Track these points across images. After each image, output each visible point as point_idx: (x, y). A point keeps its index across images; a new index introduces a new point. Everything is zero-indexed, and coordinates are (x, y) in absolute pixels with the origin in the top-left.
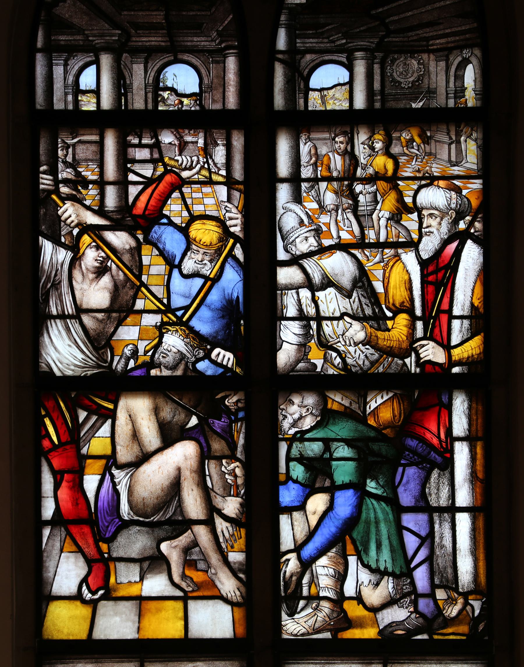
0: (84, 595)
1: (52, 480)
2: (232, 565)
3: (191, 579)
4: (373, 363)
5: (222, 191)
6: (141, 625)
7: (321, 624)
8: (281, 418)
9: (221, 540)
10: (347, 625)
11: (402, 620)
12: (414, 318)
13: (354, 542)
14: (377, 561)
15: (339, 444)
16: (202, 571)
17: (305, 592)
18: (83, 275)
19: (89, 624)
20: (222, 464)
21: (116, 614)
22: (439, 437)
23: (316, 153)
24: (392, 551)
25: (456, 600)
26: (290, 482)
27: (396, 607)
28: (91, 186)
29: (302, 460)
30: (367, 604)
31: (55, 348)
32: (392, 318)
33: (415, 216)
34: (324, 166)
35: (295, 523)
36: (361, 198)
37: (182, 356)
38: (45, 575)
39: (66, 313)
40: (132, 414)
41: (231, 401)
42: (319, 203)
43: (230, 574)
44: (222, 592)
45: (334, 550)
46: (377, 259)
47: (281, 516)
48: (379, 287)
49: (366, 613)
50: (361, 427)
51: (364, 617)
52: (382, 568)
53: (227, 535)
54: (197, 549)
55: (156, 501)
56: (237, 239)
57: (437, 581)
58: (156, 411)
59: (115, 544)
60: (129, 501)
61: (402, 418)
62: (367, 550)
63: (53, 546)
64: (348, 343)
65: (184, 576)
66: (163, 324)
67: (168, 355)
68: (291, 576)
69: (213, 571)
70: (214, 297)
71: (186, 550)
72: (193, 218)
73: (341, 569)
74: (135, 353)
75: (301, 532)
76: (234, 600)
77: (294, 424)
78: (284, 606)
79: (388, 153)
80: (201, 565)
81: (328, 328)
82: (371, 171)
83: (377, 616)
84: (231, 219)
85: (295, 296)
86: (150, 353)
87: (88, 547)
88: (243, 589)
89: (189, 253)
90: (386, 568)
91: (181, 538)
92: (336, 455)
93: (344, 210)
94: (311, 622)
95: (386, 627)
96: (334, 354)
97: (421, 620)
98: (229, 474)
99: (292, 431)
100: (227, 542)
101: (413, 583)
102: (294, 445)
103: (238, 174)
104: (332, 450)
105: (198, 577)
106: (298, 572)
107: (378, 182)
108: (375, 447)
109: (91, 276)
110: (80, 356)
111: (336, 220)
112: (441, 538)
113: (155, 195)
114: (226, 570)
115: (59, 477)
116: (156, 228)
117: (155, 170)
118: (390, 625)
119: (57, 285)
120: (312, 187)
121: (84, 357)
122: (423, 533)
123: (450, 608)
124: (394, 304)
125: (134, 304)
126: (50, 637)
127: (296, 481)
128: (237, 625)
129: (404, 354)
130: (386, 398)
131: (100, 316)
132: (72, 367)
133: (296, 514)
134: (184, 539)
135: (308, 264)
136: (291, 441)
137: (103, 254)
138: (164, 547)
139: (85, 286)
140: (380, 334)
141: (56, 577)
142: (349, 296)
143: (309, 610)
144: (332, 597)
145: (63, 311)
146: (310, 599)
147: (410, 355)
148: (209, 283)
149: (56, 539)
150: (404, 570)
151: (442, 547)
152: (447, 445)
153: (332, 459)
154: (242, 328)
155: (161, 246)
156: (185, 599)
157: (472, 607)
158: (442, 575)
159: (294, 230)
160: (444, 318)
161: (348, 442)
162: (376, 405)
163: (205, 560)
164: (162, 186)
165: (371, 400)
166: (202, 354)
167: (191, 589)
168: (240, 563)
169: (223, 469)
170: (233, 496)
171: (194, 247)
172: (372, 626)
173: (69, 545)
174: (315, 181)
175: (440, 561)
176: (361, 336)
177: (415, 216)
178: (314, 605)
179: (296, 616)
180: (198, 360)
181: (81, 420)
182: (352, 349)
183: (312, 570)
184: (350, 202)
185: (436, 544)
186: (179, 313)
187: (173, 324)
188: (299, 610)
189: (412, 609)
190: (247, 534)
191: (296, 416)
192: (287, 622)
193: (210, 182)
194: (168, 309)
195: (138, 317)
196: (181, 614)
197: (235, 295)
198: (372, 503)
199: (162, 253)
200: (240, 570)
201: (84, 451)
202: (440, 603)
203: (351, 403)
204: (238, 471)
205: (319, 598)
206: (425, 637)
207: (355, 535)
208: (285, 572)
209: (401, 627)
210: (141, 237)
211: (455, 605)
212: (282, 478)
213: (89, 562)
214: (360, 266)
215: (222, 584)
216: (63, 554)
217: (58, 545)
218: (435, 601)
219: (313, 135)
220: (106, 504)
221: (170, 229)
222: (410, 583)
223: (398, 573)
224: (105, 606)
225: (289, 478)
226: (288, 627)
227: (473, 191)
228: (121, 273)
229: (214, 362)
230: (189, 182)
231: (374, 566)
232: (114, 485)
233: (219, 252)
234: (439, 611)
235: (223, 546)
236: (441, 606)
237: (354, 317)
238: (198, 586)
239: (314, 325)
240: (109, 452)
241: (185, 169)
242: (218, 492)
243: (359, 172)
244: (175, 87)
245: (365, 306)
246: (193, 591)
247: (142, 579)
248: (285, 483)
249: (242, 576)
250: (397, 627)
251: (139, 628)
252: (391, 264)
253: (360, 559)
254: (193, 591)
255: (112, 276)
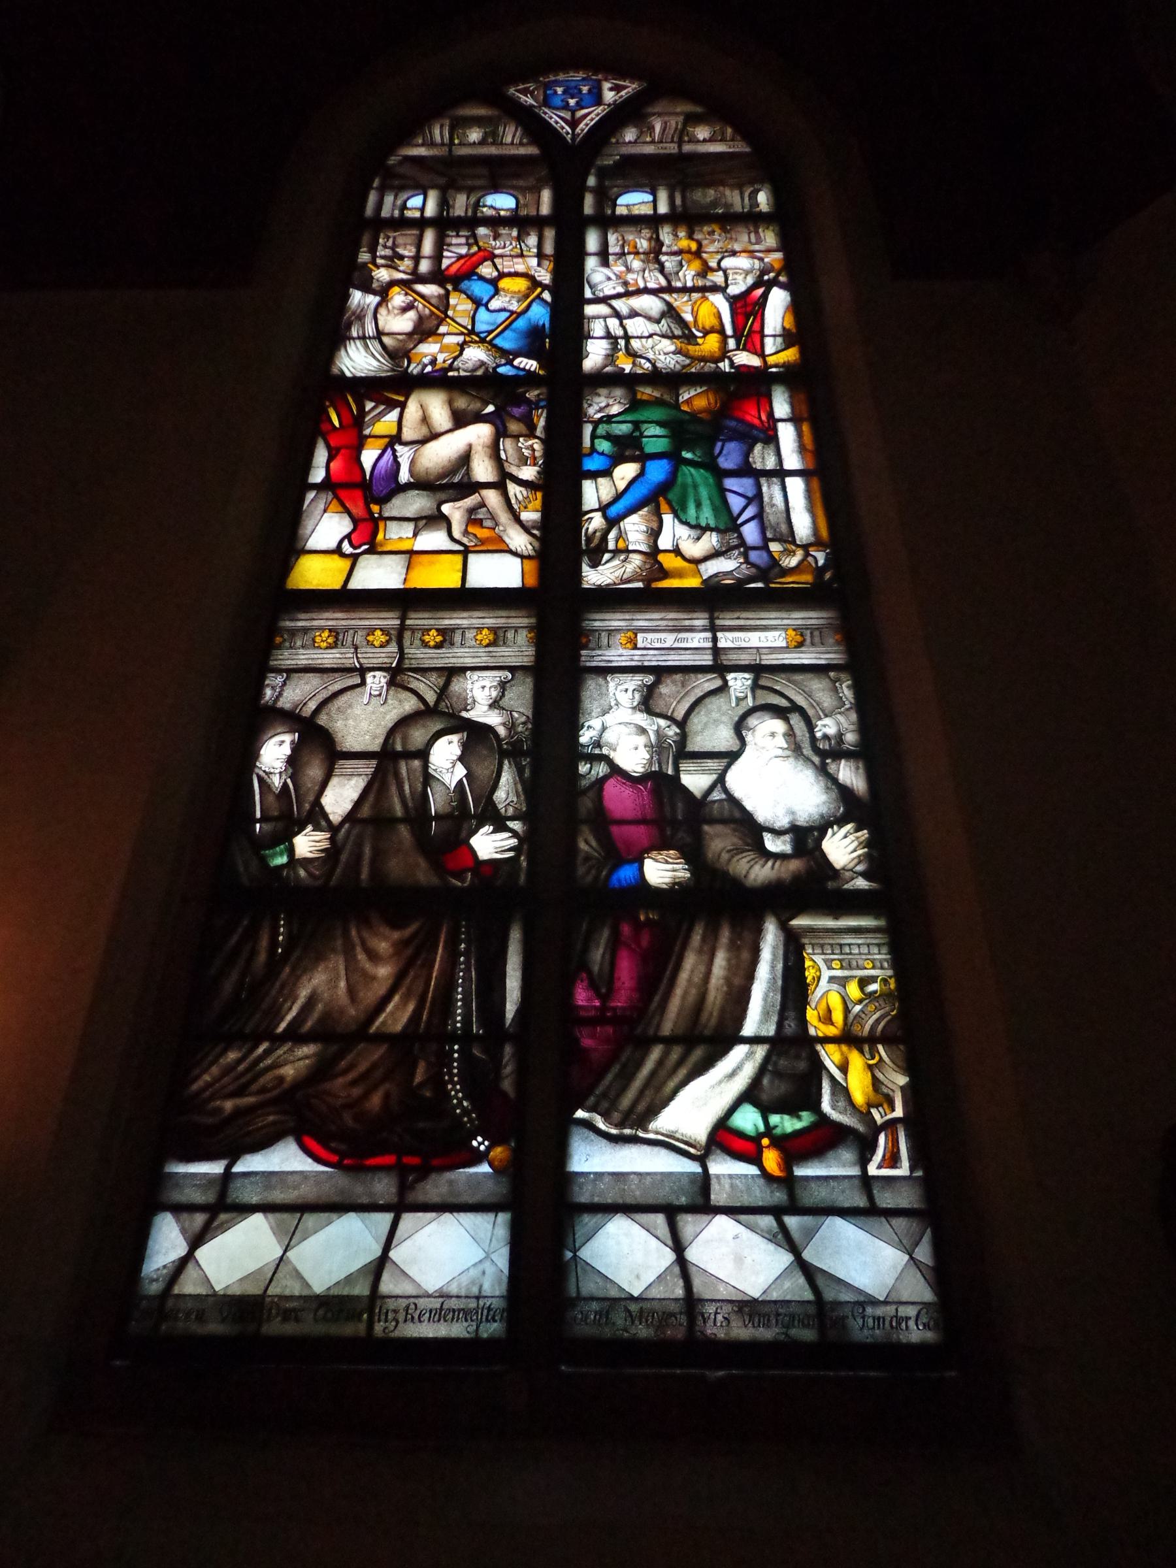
0: (344, 550)
1: (326, 454)
2: (525, 523)
3: (475, 535)
4: (684, 367)
5: (534, 262)
6: (408, 577)
7: (631, 575)
8: (585, 406)
9: (513, 501)
10: (662, 575)
11: (729, 570)
12: (724, 337)
13: (669, 503)
14: (697, 518)
15: (650, 425)
16: (488, 528)
17: (611, 545)
18: (388, 310)
19: (345, 576)
20: (519, 441)
21: (379, 567)
22: (760, 418)
23: (623, 238)
24: (715, 510)
25: (794, 552)
26: (595, 454)
27: (722, 559)
28: (406, 259)
29: (608, 437)
30: (687, 556)
31: (351, 359)
32: (704, 337)
33: (721, 273)
34: (631, 246)
35: (600, 487)
36: (667, 265)
37: (483, 364)
38: (300, 532)
39: (367, 335)
40: (424, 404)
41: (532, 395)
42: (627, 267)
43: (522, 531)
44: (511, 546)
45: (646, 509)
46: (686, 299)
47: (583, 482)
48: (688, 317)
49: (685, 564)
50: (673, 412)
51: (683, 568)
52: (703, 524)
53: (520, 497)
54: (484, 509)
55: (441, 470)
56: (545, 287)
57: (769, 535)
58: (450, 403)
59: (389, 505)
60: (411, 471)
61: (718, 405)
62: (684, 508)
63: (316, 507)
64: (657, 353)
65: (466, 533)
66: (465, 342)
67: (467, 363)
68: (595, 532)
69: (501, 528)
70: (521, 323)
71: (471, 511)
72: (502, 275)
73: (655, 526)
74: (433, 362)
75: (607, 495)
76: (525, 553)
77: (600, 410)
78: (585, 559)
79: (690, 237)
80: (488, 523)
81: (635, 344)
82: (675, 248)
83: (699, 567)
84: (539, 276)
85: (603, 323)
86: (449, 362)
87: (356, 505)
88: (536, 544)
89: (496, 297)
90: (708, 525)
91: (466, 500)
92: (646, 433)
93: (650, 271)
94: (619, 573)
95: (711, 577)
96: (643, 361)
97: (753, 570)
98: (527, 448)
99: (599, 416)
100: (520, 503)
101: (740, 536)
102: (600, 426)
103: (549, 249)
104: (643, 430)
105: (482, 533)
106: (602, 529)
107: (683, 255)
108: (692, 427)
109: (396, 312)
110: (375, 363)
111: (643, 277)
112: (771, 498)
113: (468, 263)
114: (518, 527)
115: (334, 452)
116: (466, 282)
117: (469, 249)
118: (716, 575)
119: (360, 318)
120: (620, 258)
121: (379, 364)
122: (750, 494)
123: (788, 560)
124: (703, 328)
125: (437, 328)
126: (295, 588)
127: (602, 454)
128: (526, 576)
129: (717, 360)
130: (699, 390)
131: (400, 337)
132: (366, 371)
133: (601, 480)
134: (470, 501)
135: (615, 303)
136: (596, 424)
137: (411, 298)
138: (446, 509)
139: (389, 318)
140: (690, 347)
141: (314, 534)
142: (658, 322)
143: (616, 562)
144: (644, 550)
145: (364, 334)
146: (616, 552)
147: (724, 361)
148: (514, 316)
149: (320, 501)
150: (730, 525)
151: (773, 506)
152: (769, 425)
153: (642, 436)
154: (547, 345)
155: (469, 293)
156: (466, 552)
157: (815, 558)
158: (775, 530)
159: (601, 282)
160: (757, 338)
161: (660, 424)
162: (689, 396)
163: (493, 518)
164: (474, 259)
165: (685, 392)
166: (503, 361)
167: (473, 544)
168: (534, 521)
169: (520, 445)
170: (530, 465)
171: (502, 293)
172: (693, 576)
173: (335, 505)
174: (622, 254)
175: (771, 518)
176: (672, 348)
177: (721, 273)
178: (622, 557)
179: (600, 568)
180: (498, 366)
181: (367, 409)
182: (662, 357)
183: (620, 528)
184: (657, 266)
185: (765, 503)
186: (482, 335)
187: (476, 342)
188: (603, 562)
189: (742, 560)
190: (544, 498)
191: (603, 405)
192: (588, 573)
193: (522, 255)
194: (472, 332)
195: (441, 338)
196: (460, 566)
197: (541, 323)
198: (689, 471)
199: (469, 297)
200: (534, 528)
201: (367, 432)
202: (776, 555)
203: (662, 395)
204: (536, 447)
205: (628, 551)
206: (760, 585)
207: (671, 496)
208: (588, 529)
209: (730, 577)
210: (450, 287)
211: (793, 556)
212: (586, 451)
213: (355, 521)
214: (668, 304)
215: (511, 539)
216: (326, 514)
217: (322, 506)
218: (769, 552)
219: (619, 229)
220: (383, 472)
221: (480, 283)
222: (737, 537)
223: (722, 527)
224: (367, 559)
225: (593, 450)
226: (589, 578)
227: (775, 260)
228: (427, 310)
229: (518, 368)
230: (501, 256)
231: (693, 522)
232: (395, 457)
233: (527, 296)
234: (774, 562)
235: (516, 507)
236: (777, 557)
237: (663, 336)
238: (483, 542)
239: (622, 342)
240: (394, 431)
241: (499, 248)
242: (513, 462)
243: (664, 249)
244: (494, 205)
245: (673, 329)
246: (476, 545)
247: (415, 535)
248: (590, 454)
249: (535, 532)
250: (724, 577)
251: (405, 579)
252: (699, 303)
253: (676, 516)
254: (476, 545)
255: (418, 311)
